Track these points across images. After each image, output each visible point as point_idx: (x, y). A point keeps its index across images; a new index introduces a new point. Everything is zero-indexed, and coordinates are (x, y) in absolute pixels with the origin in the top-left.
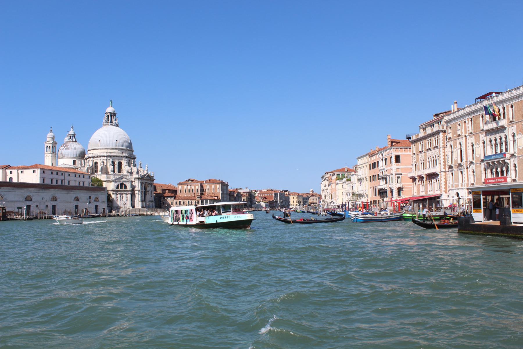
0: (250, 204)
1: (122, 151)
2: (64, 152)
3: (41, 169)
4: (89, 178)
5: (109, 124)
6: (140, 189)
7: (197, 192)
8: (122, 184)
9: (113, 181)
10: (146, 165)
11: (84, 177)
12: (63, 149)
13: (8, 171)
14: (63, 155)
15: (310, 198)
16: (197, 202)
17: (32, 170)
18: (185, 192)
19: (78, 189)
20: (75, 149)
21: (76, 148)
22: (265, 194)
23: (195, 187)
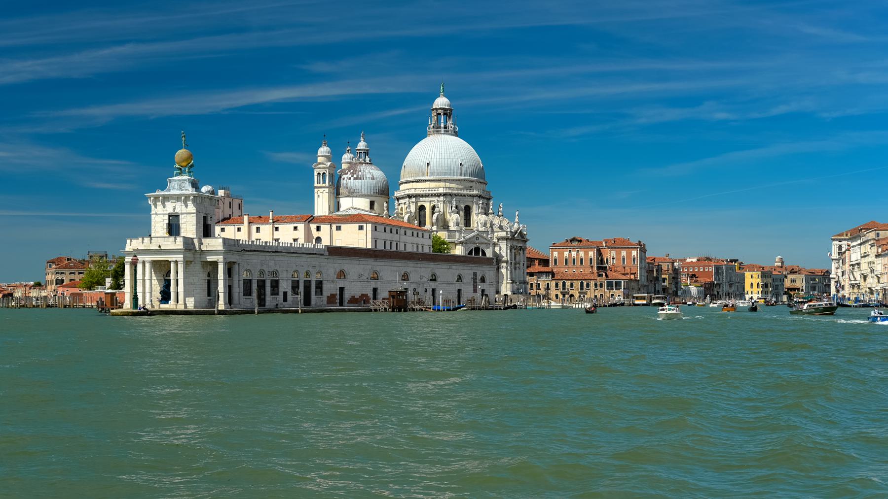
0: (675, 289)
1: (471, 184)
2: (352, 185)
3: (372, 223)
4: (430, 238)
5: (443, 132)
6: (509, 260)
7: (591, 263)
8: (477, 250)
9: (461, 243)
10: (517, 213)
11: (423, 237)
12: (350, 179)
13: (313, 227)
14: (349, 190)
15: (786, 277)
16: (599, 284)
17: (356, 226)
18: (566, 263)
19: (461, 262)
20: (373, 178)
21: (375, 176)
22: (693, 267)
23: (586, 254)
